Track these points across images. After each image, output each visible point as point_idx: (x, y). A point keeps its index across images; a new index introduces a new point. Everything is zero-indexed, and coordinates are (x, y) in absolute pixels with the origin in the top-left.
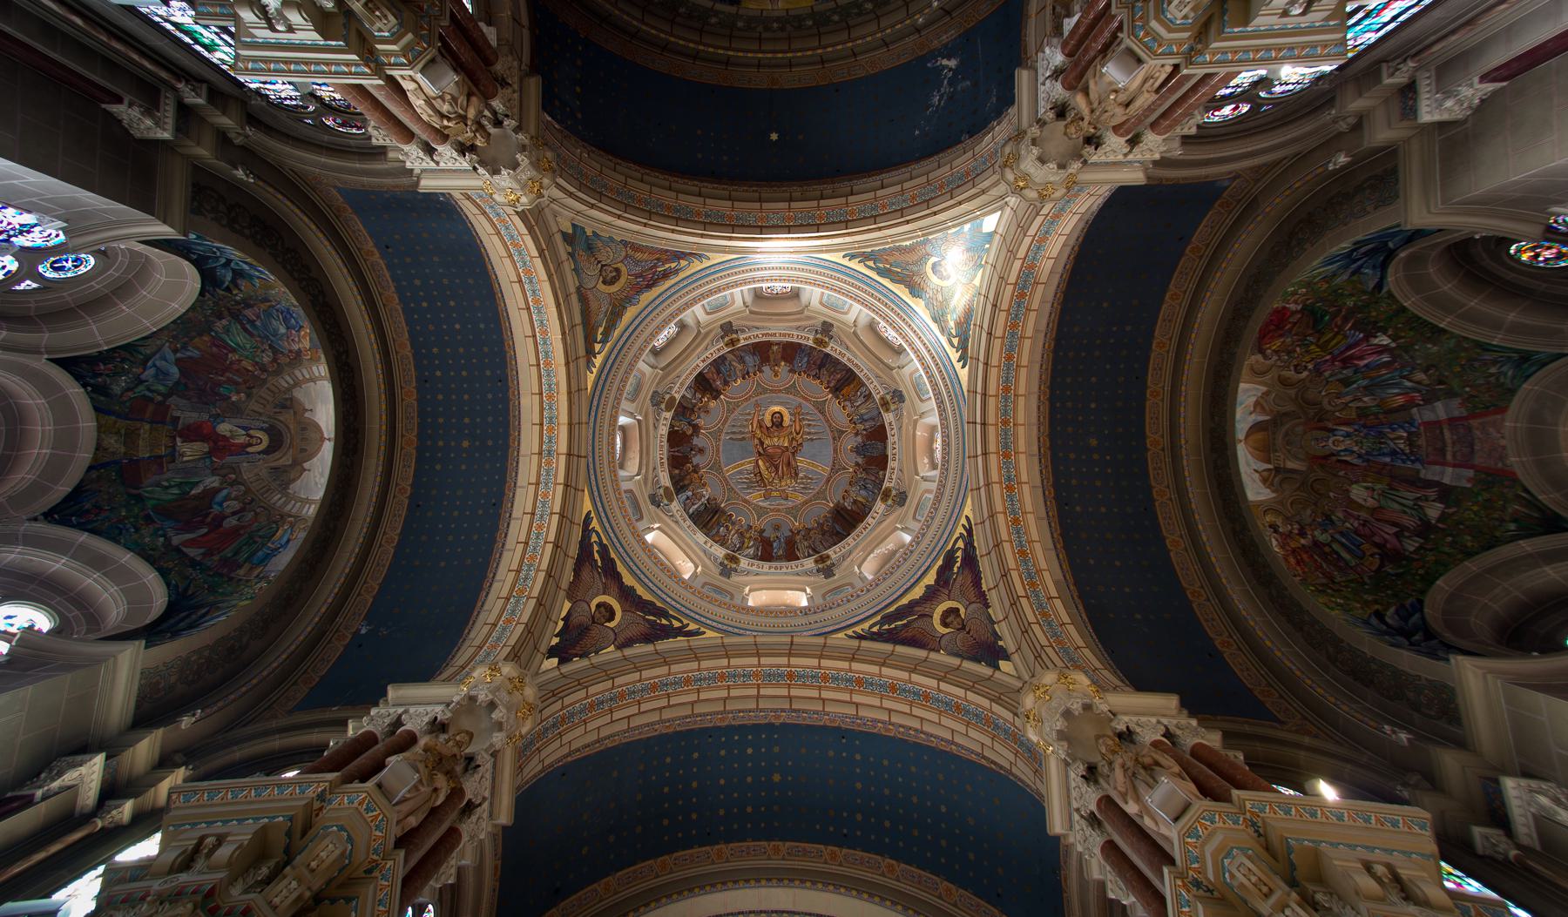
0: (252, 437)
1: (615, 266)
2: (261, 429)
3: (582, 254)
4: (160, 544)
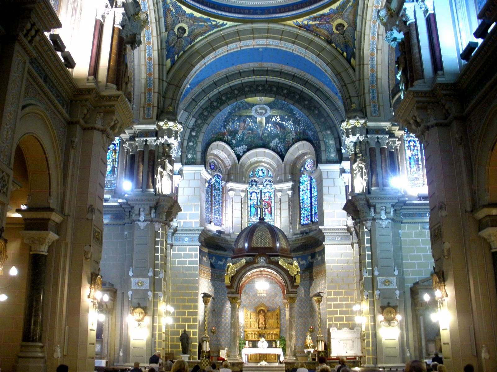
1: (337, 32)
3: (350, 44)
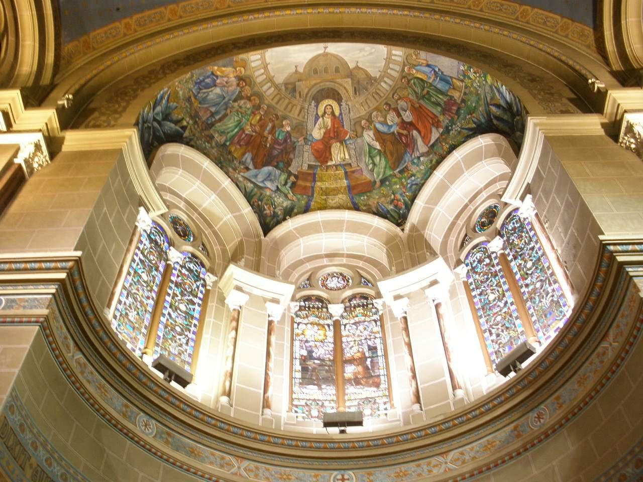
0: (325, 113)
2: (317, 106)
4: (426, 159)
